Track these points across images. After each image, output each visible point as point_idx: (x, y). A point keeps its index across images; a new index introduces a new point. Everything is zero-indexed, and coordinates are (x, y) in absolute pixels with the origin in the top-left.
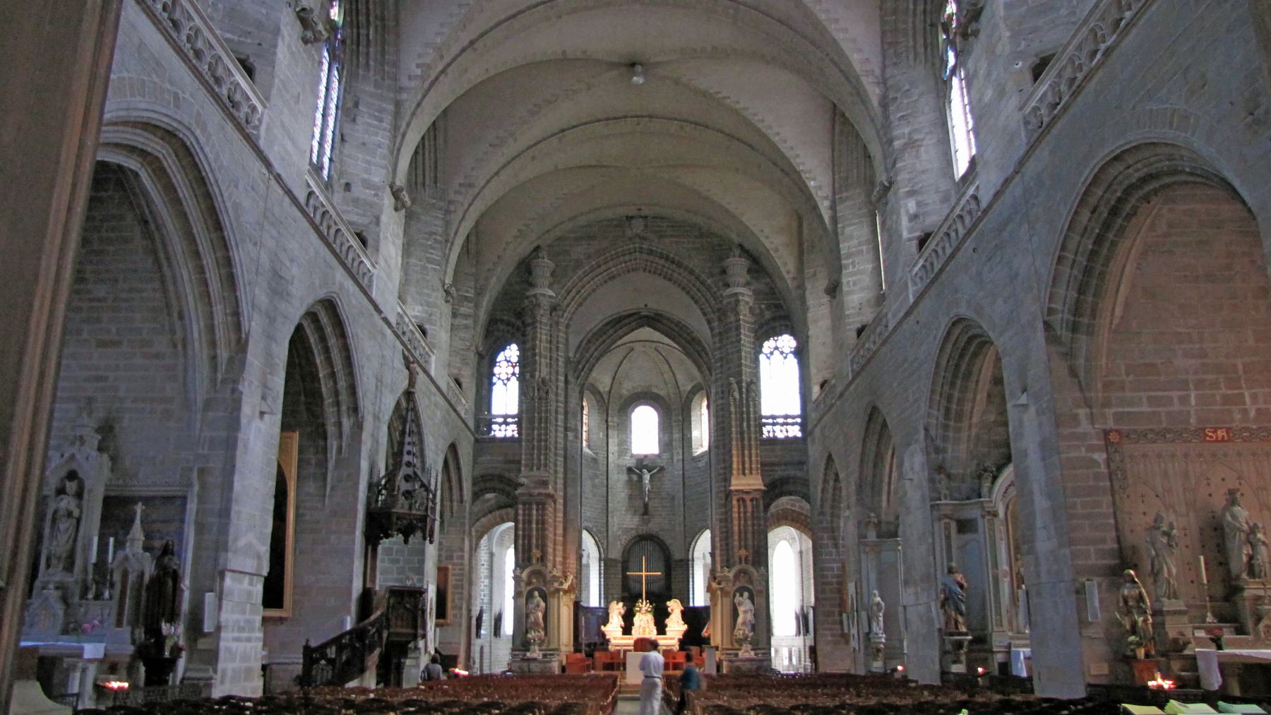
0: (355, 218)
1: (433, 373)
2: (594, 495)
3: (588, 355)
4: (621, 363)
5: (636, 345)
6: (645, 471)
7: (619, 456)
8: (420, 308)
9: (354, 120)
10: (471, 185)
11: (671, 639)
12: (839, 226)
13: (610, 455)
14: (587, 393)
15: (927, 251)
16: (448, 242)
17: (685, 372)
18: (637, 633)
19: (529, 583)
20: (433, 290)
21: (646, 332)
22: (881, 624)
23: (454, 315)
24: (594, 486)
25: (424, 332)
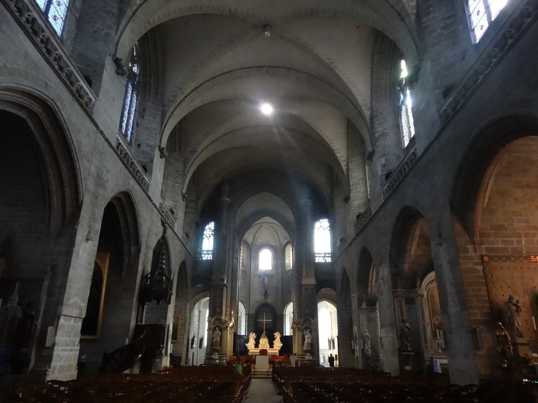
0: (142, 159)
1: (176, 230)
4: (257, 231)
5: (264, 225)
8: (171, 202)
9: (143, 117)
10: (195, 152)
12: (350, 172)
14: (242, 243)
15: (391, 179)
16: (185, 175)
17: (283, 235)
18: (261, 347)
19: (214, 324)
20: (177, 195)
21: (268, 219)
22: (369, 345)
23: (187, 207)
25: (173, 213)
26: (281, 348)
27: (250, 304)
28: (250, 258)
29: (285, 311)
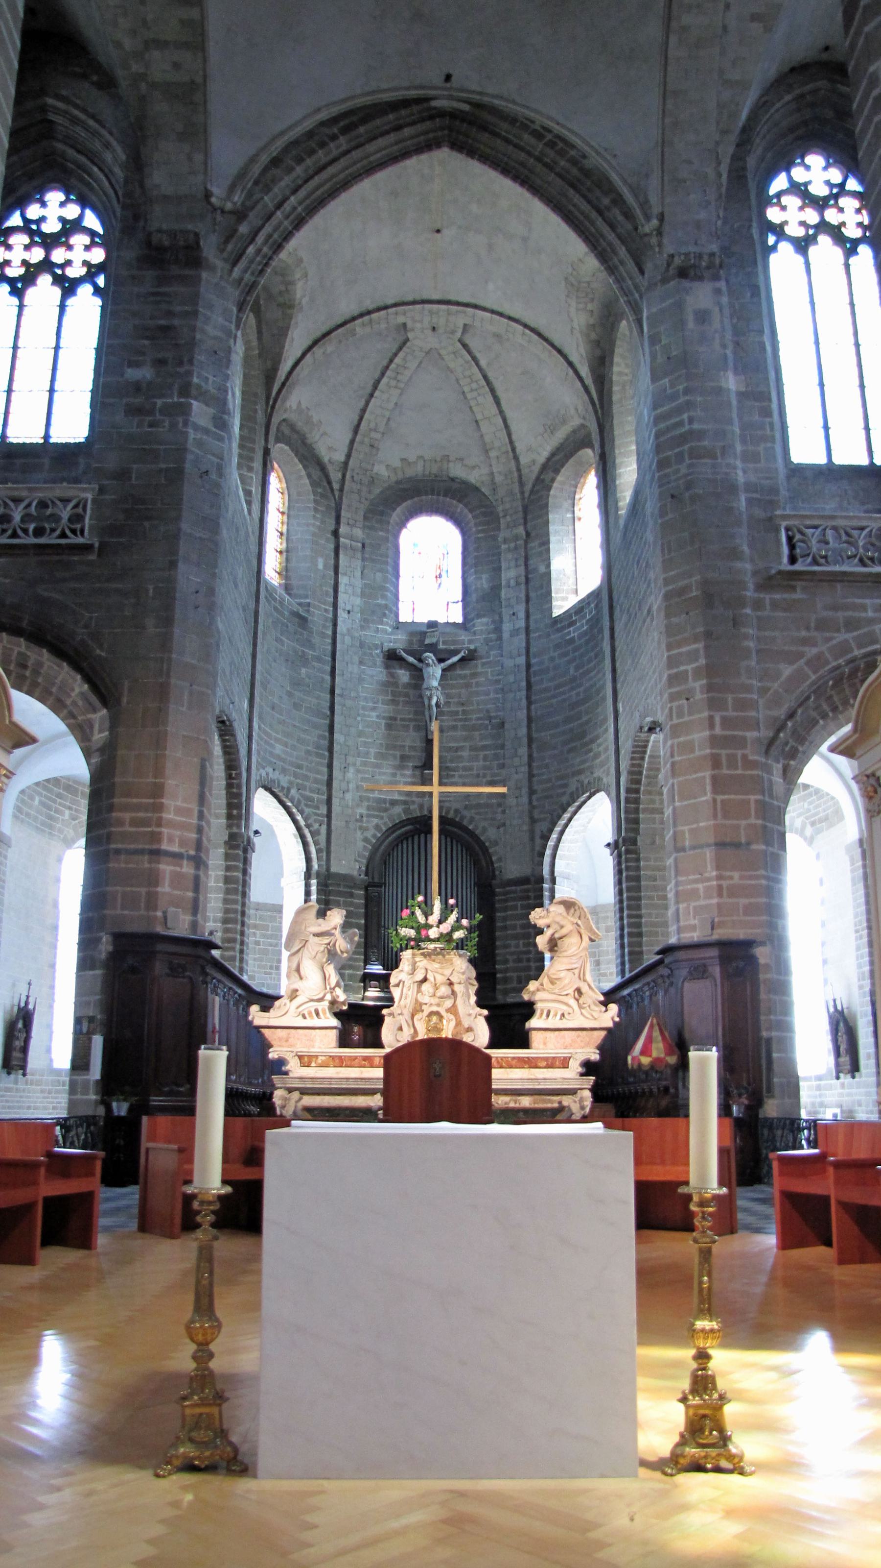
2: (296, 706)
3: (268, 200)
4: (375, 386)
6: (430, 657)
7: (365, 623)
11: (551, 1063)
13: (342, 615)
24: (297, 683)
26: (601, 1048)
27: (333, 815)
28: (332, 546)
29: (548, 852)
